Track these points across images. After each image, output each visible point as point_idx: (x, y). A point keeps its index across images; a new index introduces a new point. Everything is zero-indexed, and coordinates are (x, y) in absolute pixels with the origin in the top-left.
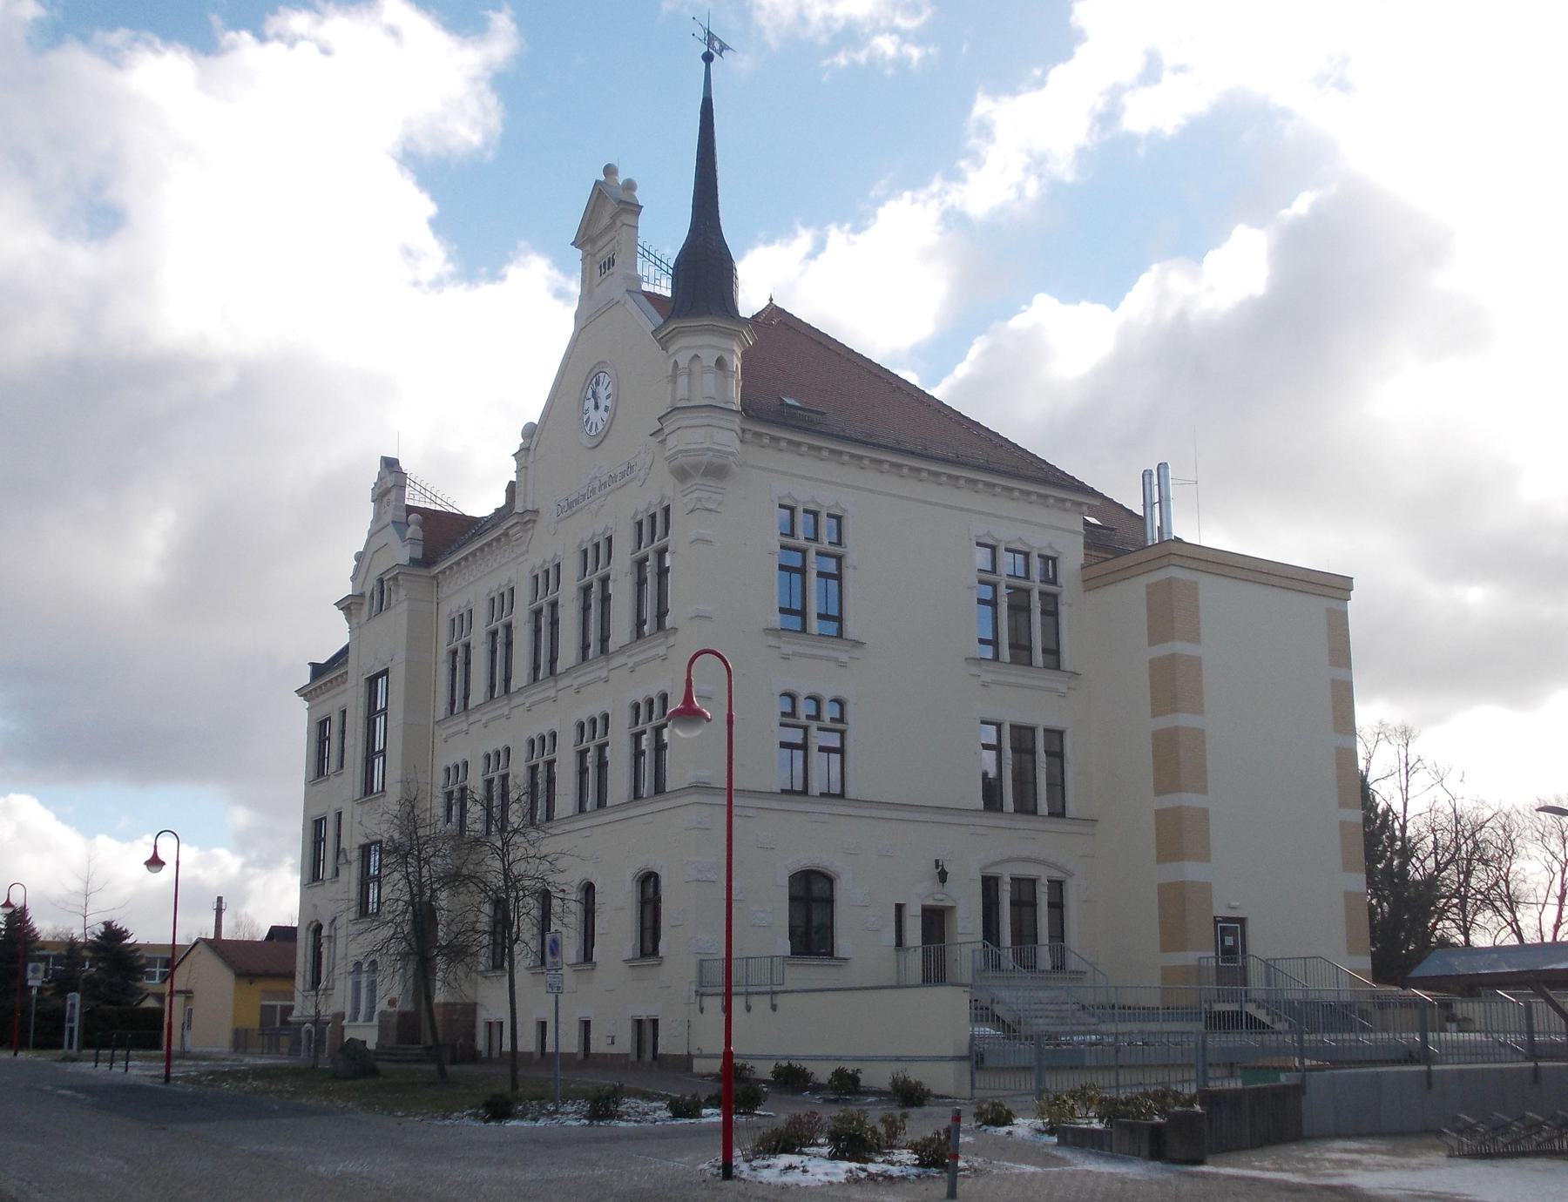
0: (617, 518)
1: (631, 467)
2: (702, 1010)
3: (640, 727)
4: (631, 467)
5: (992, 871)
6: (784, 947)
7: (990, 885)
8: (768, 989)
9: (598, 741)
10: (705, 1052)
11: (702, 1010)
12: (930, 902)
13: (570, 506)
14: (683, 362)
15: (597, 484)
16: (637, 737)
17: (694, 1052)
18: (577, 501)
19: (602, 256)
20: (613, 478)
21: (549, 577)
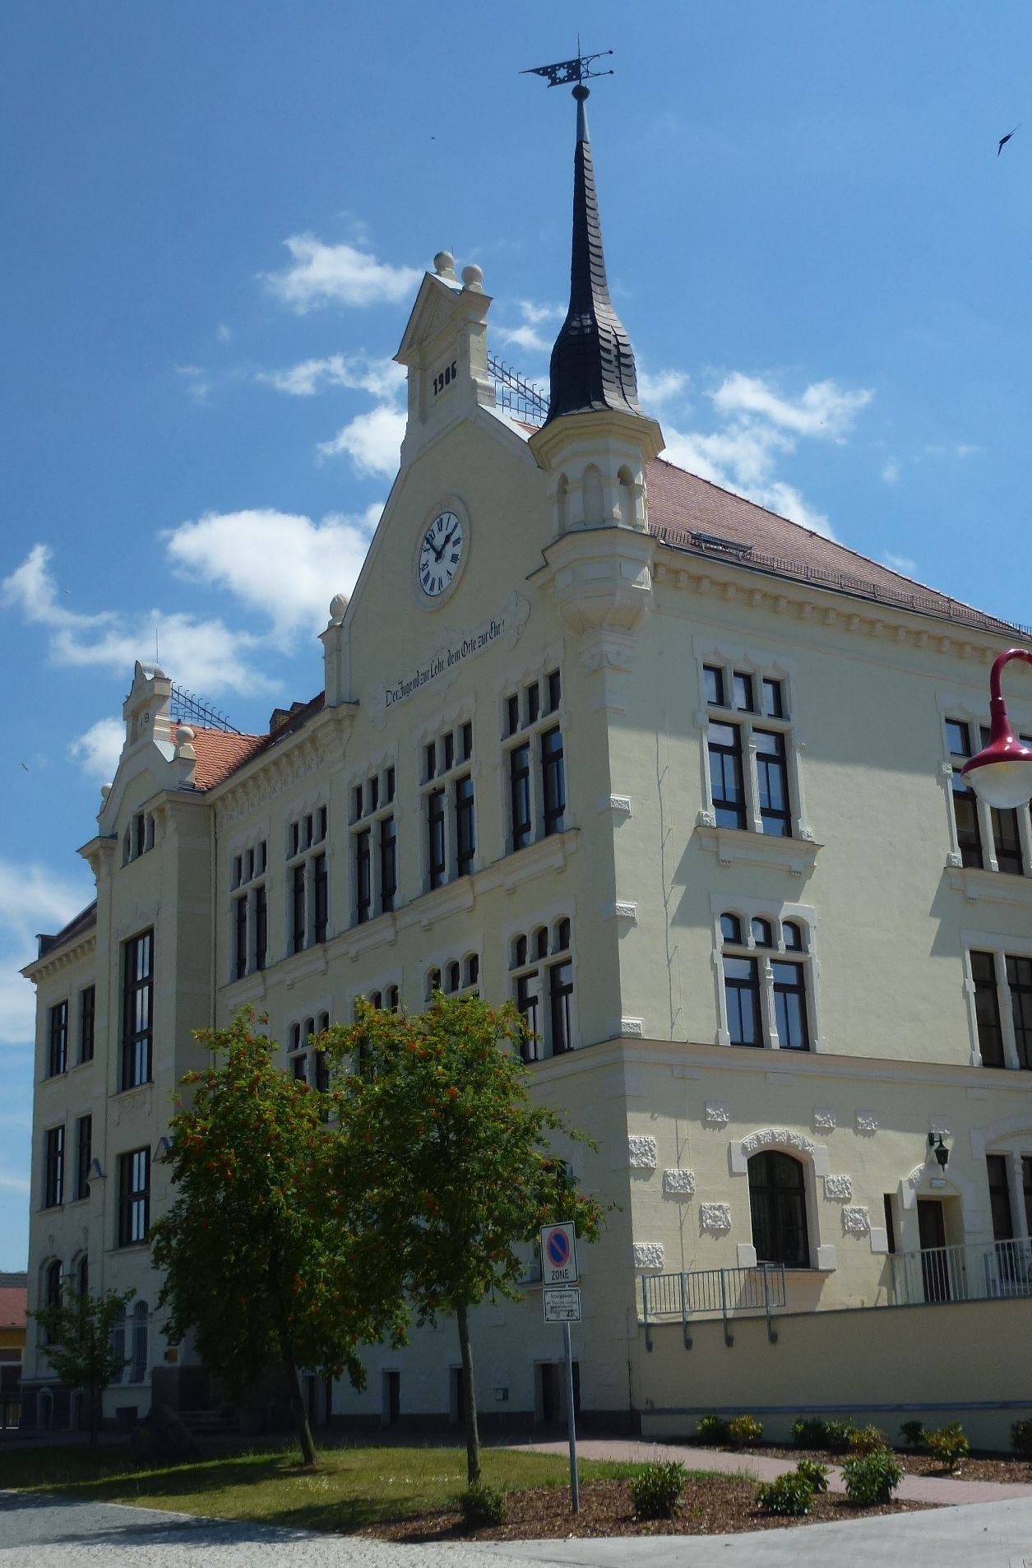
0: (477, 697)
1: (495, 629)
2: (649, 1347)
3: (528, 966)
4: (495, 629)
5: (999, 1149)
6: (749, 1257)
7: (997, 1164)
8: (762, 1312)
9: (551, 958)
10: (657, 1406)
11: (649, 1347)
12: (930, 1193)
13: (406, 690)
14: (574, 470)
15: (444, 656)
16: (521, 983)
17: (640, 1405)
18: (416, 683)
19: (439, 367)
20: (469, 645)
21: (377, 789)
